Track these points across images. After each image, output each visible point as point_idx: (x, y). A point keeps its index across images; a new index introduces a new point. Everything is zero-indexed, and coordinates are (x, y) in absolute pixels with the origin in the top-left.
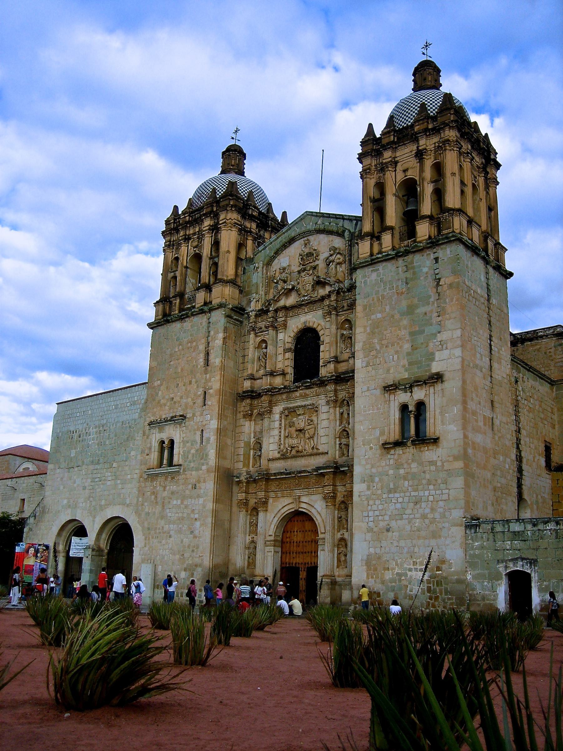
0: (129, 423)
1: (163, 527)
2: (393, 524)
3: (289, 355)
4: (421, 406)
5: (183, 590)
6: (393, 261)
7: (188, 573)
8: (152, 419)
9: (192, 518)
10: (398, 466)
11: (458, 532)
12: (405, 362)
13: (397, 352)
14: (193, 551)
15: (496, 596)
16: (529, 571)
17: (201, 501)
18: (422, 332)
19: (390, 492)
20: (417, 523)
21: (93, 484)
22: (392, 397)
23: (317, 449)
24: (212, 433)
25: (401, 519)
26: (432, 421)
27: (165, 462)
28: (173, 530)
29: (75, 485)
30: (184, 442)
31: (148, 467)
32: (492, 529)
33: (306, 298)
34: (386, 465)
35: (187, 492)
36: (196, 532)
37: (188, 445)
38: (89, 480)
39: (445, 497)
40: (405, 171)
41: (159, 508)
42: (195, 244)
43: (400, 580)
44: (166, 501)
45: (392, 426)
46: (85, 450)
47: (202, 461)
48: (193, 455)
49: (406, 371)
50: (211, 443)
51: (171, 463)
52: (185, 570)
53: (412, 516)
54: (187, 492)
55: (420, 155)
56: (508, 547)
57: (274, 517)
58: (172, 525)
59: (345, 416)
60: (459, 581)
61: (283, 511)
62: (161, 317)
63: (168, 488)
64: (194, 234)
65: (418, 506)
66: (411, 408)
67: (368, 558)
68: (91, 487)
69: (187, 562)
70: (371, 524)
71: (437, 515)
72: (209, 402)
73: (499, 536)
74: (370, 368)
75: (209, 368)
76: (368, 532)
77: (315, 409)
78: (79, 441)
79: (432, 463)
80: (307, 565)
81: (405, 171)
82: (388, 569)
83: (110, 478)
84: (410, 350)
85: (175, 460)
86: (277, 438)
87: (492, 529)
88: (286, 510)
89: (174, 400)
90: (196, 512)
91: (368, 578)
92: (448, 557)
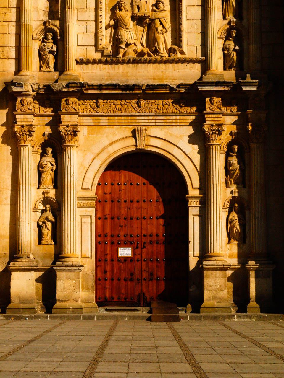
23: (182, 53)
57: (93, 160)
61: (111, 149)
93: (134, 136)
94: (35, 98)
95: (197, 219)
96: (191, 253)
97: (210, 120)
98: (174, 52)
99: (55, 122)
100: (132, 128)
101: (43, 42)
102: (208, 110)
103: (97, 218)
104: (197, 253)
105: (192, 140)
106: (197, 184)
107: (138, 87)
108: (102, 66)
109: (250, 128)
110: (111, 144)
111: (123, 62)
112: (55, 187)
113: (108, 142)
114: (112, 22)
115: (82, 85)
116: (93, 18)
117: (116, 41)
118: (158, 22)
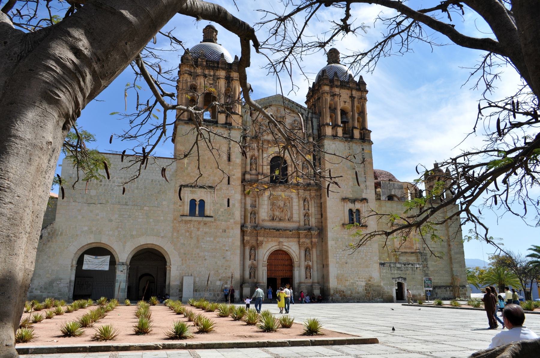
0: (159, 181)
1: (198, 254)
2: (348, 260)
4: (358, 211)
6: (343, 143)
7: (222, 282)
8: (183, 183)
11: (377, 266)
13: (346, 184)
14: (226, 269)
15: (392, 292)
17: (230, 240)
20: (359, 261)
21: (121, 218)
22: (346, 204)
24: (237, 202)
25: (352, 259)
27: (197, 212)
29: (98, 217)
30: (214, 203)
31: (181, 213)
32: (390, 265)
33: (281, 140)
37: (219, 205)
38: (117, 216)
39: (371, 251)
40: (345, 102)
42: (212, 82)
43: (353, 286)
45: (346, 217)
46: (109, 193)
47: (229, 217)
49: (351, 194)
50: (236, 206)
51: (202, 214)
52: (220, 280)
53: (357, 258)
54: (219, 234)
55: (352, 97)
59: (307, 206)
60: (378, 286)
61: (272, 249)
62: (186, 119)
63: (201, 229)
64: (211, 76)
66: (354, 211)
67: (337, 276)
68: (119, 221)
70: (338, 260)
72: (233, 183)
75: (232, 163)
76: (337, 263)
78: (101, 185)
80: (281, 277)
81: (345, 102)
83: (142, 217)
84: (352, 185)
85: (208, 212)
86: (266, 210)
87: (390, 265)
88: (274, 248)
91: (338, 284)
97: (301, 240)
103: (268, 270)
107: (281, 229)
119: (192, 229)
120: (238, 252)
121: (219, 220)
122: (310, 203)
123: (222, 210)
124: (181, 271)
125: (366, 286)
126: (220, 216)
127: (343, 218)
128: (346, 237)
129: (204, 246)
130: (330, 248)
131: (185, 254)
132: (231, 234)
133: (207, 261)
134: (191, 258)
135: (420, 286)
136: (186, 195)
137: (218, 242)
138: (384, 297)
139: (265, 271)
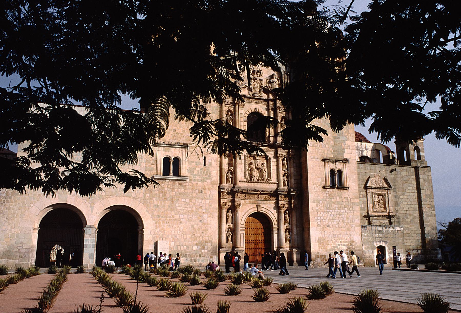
1: (173, 216)
2: (330, 223)
3: (246, 124)
5: (196, 258)
7: (199, 247)
9: (201, 212)
10: (331, 197)
12: (331, 149)
13: (327, 144)
14: (203, 232)
16: (385, 246)
17: (207, 201)
18: (339, 138)
19: (328, 208)
23: (271, 180)
25: (334, 222)
26: (345, 179)
28: (183, 218)
32: (371, 229)
34: (325, 196)
35: (195, 195)
36: (205, 221)
39: (352, 214)
41: (168, 203)
44: (175, 198)
47: (206, 176)
48: (198, 171)
49: (332, 154)
50: (213, 166)
52: (197, 245)
56: (377, 236)
58: (182, 216)
60: (359, 250)
61: (250, 211)
63: (176, 190)
65: (341, 216)
69: (198, 240)
70: (319, 223)
71: (349, 221)
73: (374, 231)
74: (315, 148)
77: (267, 158)
79: (346, 198)
82: (329, 245)
84: (333, 145)
87: (371, 229)
89: (177, 131)
90: (203, 208)
91: (319, 249)
92: (355, 240)
93: (257, 207)
94: (226, 193)
95: (276, 235)
96: (274, 246)
97: (280, 203)
98: (269, 180)
99: (233, 201)
100: (256, 204)
101: (227, 174)
102: (280, 200)
104: (276, 246)
105: (275, 208)
106: (276, 223)
107: (260, 191)
108: (247, 183)
109: (293, 206)
110: (250, 210)
111: (253, 182)
112: (232, 223)
113: (249, 209)
114: (249, 169)
115: (243, 190)
116: (244, 167)
117: (251, 176)
118: (263, 170)
119: (167, 189)
120: (216, 214)
121: (195, 180)
122: (289, 162)
123: (198, 169)
124: (155, 235)
125: (347, 250)
126: (196, 175)
127: (325, 179)
128: (328, 200)
129: (180, 208)
130: (310, 210)
131: (159, 216)
132: (208, 196)
133: (182, 224)
134: (165, 221)
135: (400, 250)
136: (159, 152)
137: (194, 204)
138: (365, 261)
139: (242, 235)
